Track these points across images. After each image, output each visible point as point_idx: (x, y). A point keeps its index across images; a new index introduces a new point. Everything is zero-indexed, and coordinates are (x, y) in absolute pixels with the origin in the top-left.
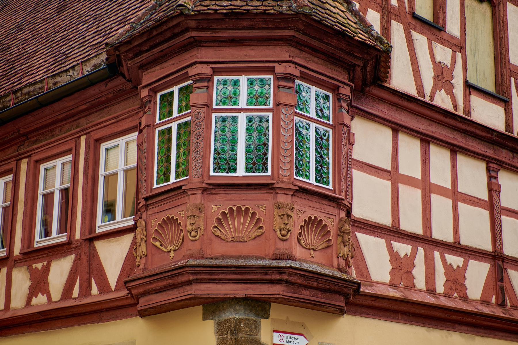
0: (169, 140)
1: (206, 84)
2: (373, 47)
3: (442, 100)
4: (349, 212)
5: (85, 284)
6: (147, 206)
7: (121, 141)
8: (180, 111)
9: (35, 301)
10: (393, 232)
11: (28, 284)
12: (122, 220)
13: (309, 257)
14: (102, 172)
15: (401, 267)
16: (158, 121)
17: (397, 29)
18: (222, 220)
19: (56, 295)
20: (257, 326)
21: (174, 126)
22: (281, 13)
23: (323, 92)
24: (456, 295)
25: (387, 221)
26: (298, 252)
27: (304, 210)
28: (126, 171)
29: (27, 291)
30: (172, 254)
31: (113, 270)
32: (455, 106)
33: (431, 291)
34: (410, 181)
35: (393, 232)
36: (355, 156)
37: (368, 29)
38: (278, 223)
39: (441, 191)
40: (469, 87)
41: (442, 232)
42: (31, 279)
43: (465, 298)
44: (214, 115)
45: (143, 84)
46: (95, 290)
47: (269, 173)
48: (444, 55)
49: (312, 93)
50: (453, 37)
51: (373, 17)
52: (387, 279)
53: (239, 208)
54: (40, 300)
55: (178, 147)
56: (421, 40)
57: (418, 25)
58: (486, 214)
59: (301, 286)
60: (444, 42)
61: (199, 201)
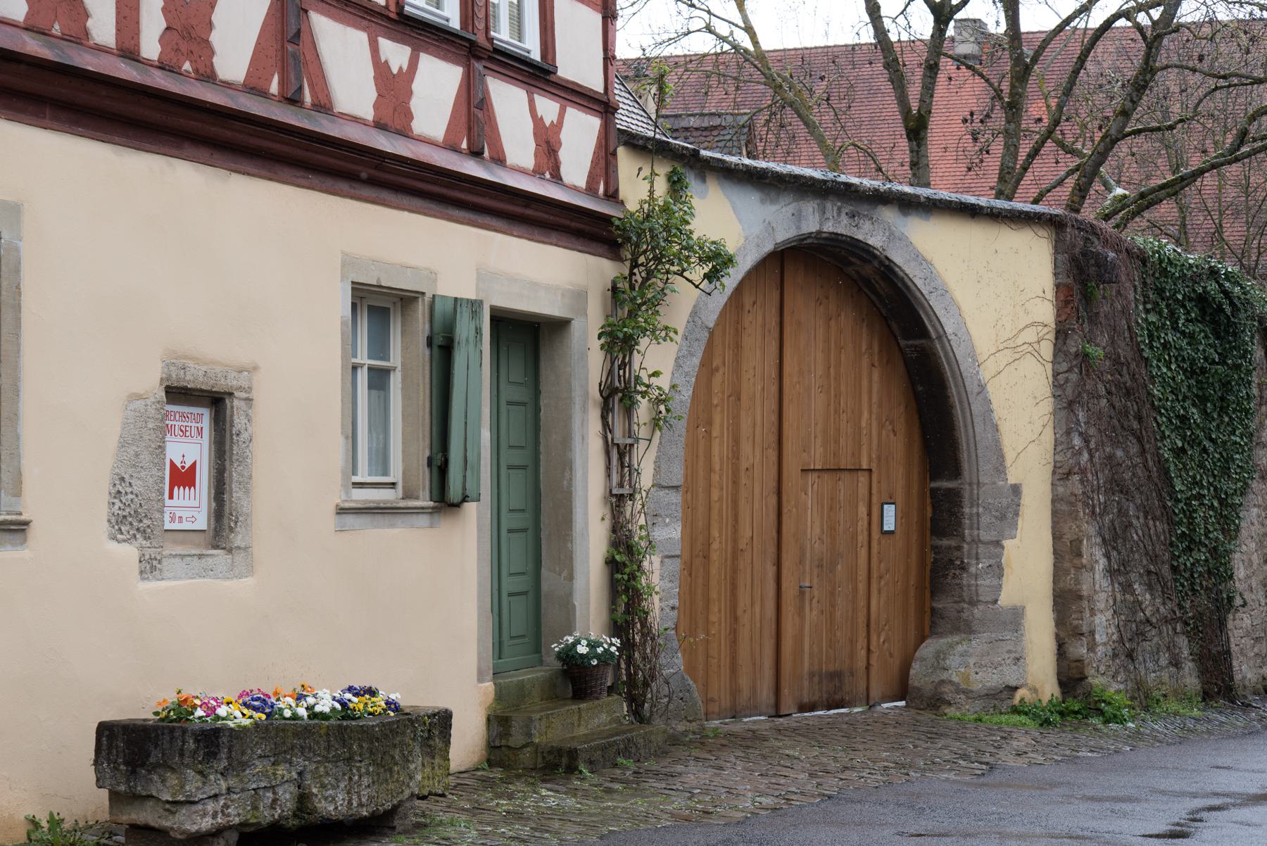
24: (187, 66)
33: (129, 52)
43: (208, 76)
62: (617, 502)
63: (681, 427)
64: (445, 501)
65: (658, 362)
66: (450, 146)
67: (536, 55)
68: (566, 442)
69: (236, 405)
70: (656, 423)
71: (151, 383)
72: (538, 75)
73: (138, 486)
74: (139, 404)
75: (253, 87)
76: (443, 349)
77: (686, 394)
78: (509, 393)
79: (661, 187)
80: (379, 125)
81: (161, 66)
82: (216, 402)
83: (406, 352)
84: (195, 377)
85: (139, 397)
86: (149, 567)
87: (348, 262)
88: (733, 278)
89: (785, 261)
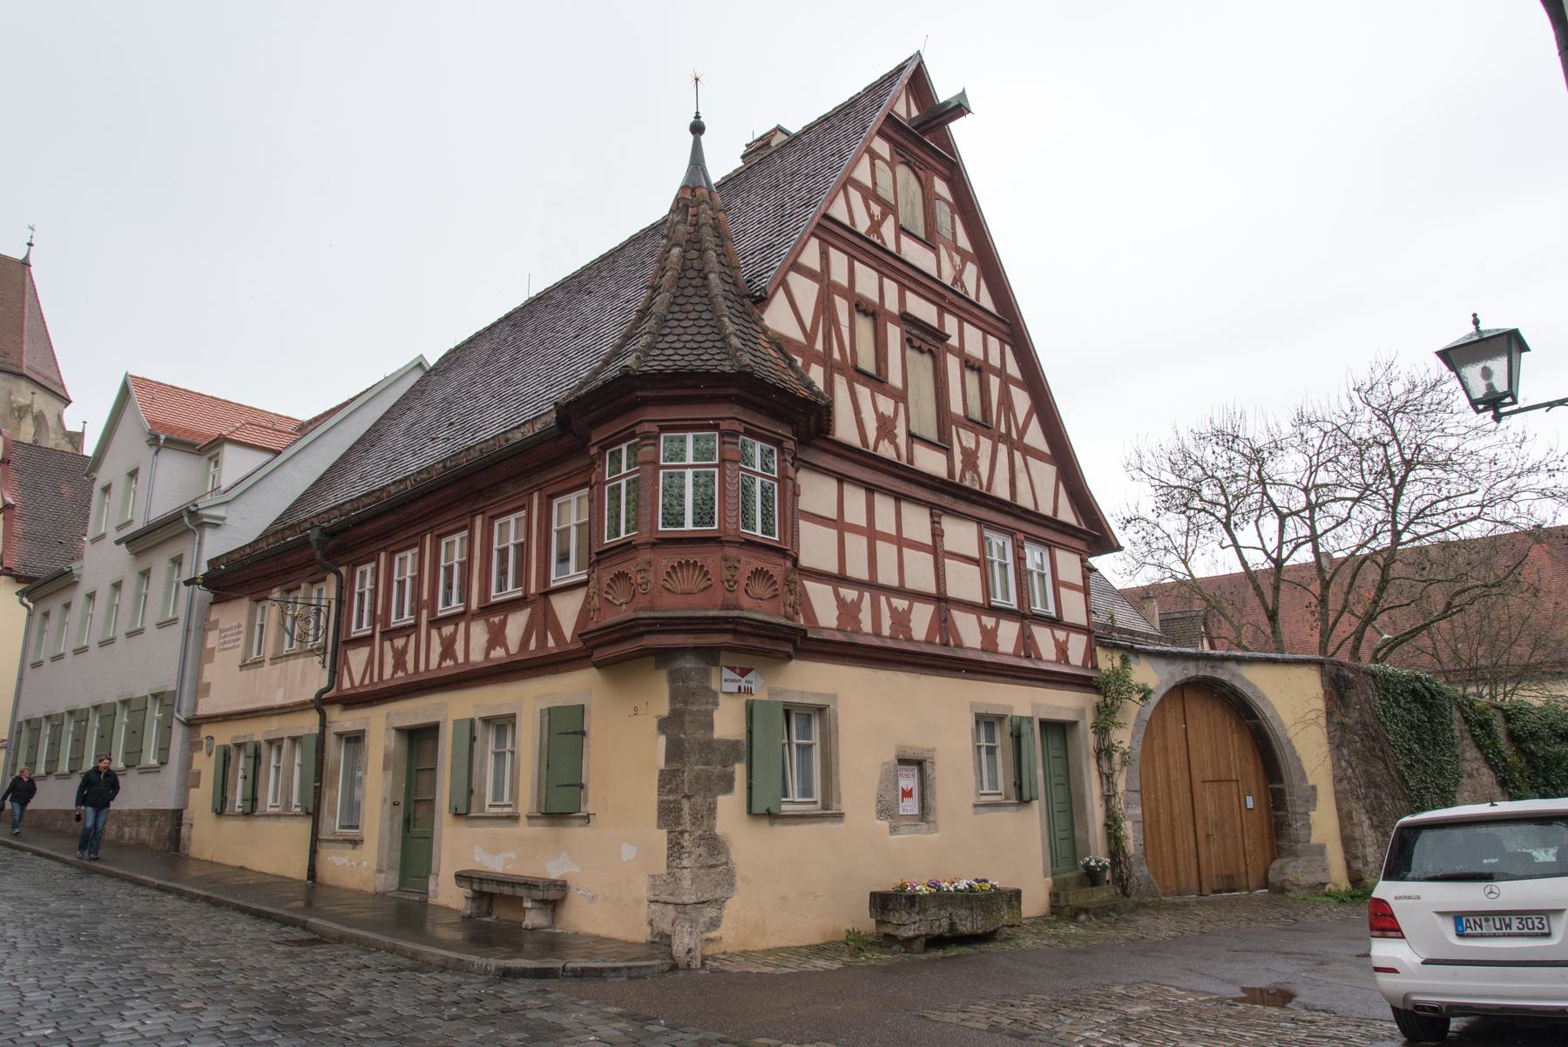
0: (619, 497)
2: (815, 403)
3: (886, 450)
4: (795, 561)
6: (598, 561)
7: (573, 497)
8: (629, 467)
9: (493, 654)
10: (839, 579)
12: (574, 573)
13: (757, 607)
14: (555, 527)
15: (848, 612)
17: (840, 383)
19: (513, 649)
20: (707, 675)
21: (623, 482)
22: (723, 372)
23: (768, 446)
25: (833, 568)
26: (746, 601)
27: (750, 562)
28: (578, 526)
31: (568, 627)
32: (898, 456)
33: (877, 634)
34: (855, 529)
35: (839, 579)
37: (810, 385)
38: (726, 574)
39: (886, 537)
40: (912, 436)
41: (888, 576)
43: (910, 639)
46: (551, 643)
48: (886, 405)
49: (757, 448)
50: (895, 388)
51: (816, 374)
52: (834, 624)
55: (628, 503)
56: (864, 392)
57: (861, 378)
58: (930, 557)
62: (1107, 799)
63: (1137, 764)
64: (1023, 800)
65: (1124, 737)
66: (1016, 655)
67: (1054, 614)
68: (1081, 773)
69: (928, 765)
70: (1124, 763)
71: (891, 757)
72: (1055, 622)
75: (929, 641)
76: (1017, 737)
77: (1139, 750)
78: (1053, 753)
79: (1117, 663)
80: (983, 650)
81: (891, 637)
82: (920, 764)
83: (1002, 739)
84: (909, 754)
86: (894, 830)
87: (972, 705)
88: (1154, 700)
89: (1182, 690)
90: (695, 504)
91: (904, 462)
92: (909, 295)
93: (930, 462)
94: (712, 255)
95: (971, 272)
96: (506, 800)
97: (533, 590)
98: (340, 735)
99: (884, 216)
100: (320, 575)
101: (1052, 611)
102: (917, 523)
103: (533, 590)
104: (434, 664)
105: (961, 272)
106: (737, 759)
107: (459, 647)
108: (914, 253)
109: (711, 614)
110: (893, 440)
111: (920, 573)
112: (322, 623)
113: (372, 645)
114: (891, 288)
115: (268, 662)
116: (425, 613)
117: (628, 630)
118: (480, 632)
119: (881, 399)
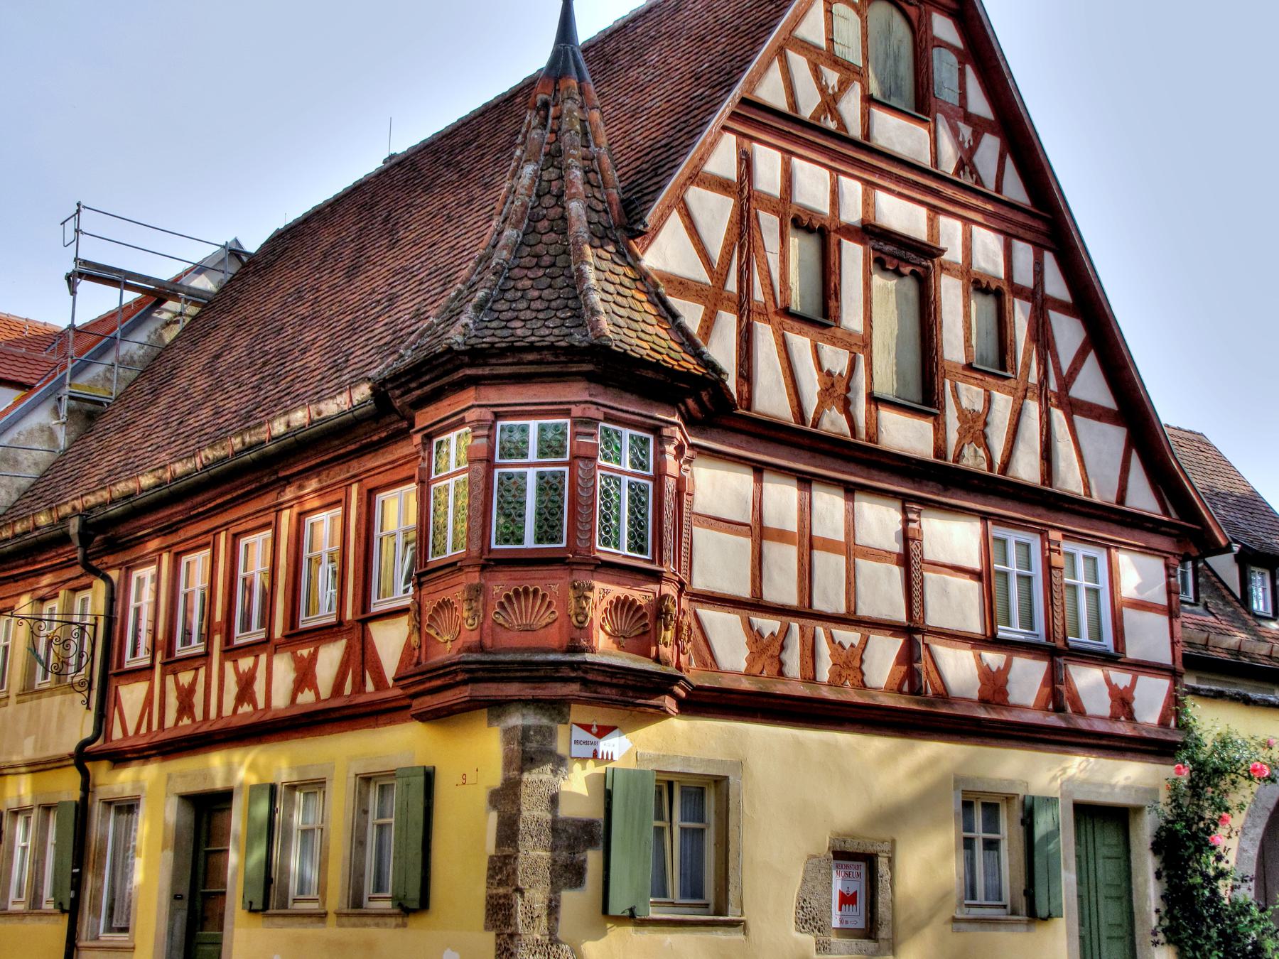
1: (486, 432)
5: (359, 679)
11: (292, 676)
15: (766, 651)
16: (433, 476)
18: (506, 605)
19: (325, 691)
20: (550, 734)
25: (745, 592)
29: (291, 686)
30: (449, 645)
35: (756, 605)
36: (697, 509)
42: (297, 669)
44: (497, 471)
45: (417, 428)
46: (370, 687)
47: (564, 544)
48: (837, 360)
52: (742, 666)
53: (526, 591)
54: (306, 697)
56: (801, 344)
58: (897, 572)
59: (602, 684)
60: (833, 341)
61: (477, 581)
71: (824, 848)
73: (814, 904)
74: (815, 861)
82: (870, 860)
84: (851, 847)
85: (815, 857)
90: (539, 514)
91: (862, 439)
92: (882, 198)
93: (905, 434)
94: (577, 174)
95: (990, 146)
96: (314, 894)
97: (349, 615)
98: (108, 803)
99: (844, 85)
100: (85, 581)
101: (1108, 642)
102: (879, 521)
103: (349, 615)
104: (228, 709)
105: (972, 150)
106: (591, 843)
107: (259, 687)
108: (896, 134)
109: (552, 657)
110: (847, 407)
111: (882, 593)
112: (87, 647)
113: (151, 680)
114: (852, 189)
115: (13, 699)
116: (217, 640)
117: (449, 674)
118: (283, 668)
119: (827, 350)
